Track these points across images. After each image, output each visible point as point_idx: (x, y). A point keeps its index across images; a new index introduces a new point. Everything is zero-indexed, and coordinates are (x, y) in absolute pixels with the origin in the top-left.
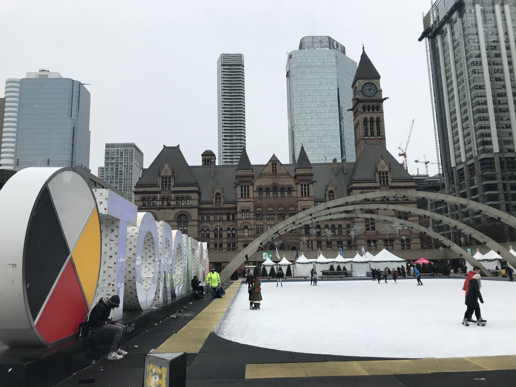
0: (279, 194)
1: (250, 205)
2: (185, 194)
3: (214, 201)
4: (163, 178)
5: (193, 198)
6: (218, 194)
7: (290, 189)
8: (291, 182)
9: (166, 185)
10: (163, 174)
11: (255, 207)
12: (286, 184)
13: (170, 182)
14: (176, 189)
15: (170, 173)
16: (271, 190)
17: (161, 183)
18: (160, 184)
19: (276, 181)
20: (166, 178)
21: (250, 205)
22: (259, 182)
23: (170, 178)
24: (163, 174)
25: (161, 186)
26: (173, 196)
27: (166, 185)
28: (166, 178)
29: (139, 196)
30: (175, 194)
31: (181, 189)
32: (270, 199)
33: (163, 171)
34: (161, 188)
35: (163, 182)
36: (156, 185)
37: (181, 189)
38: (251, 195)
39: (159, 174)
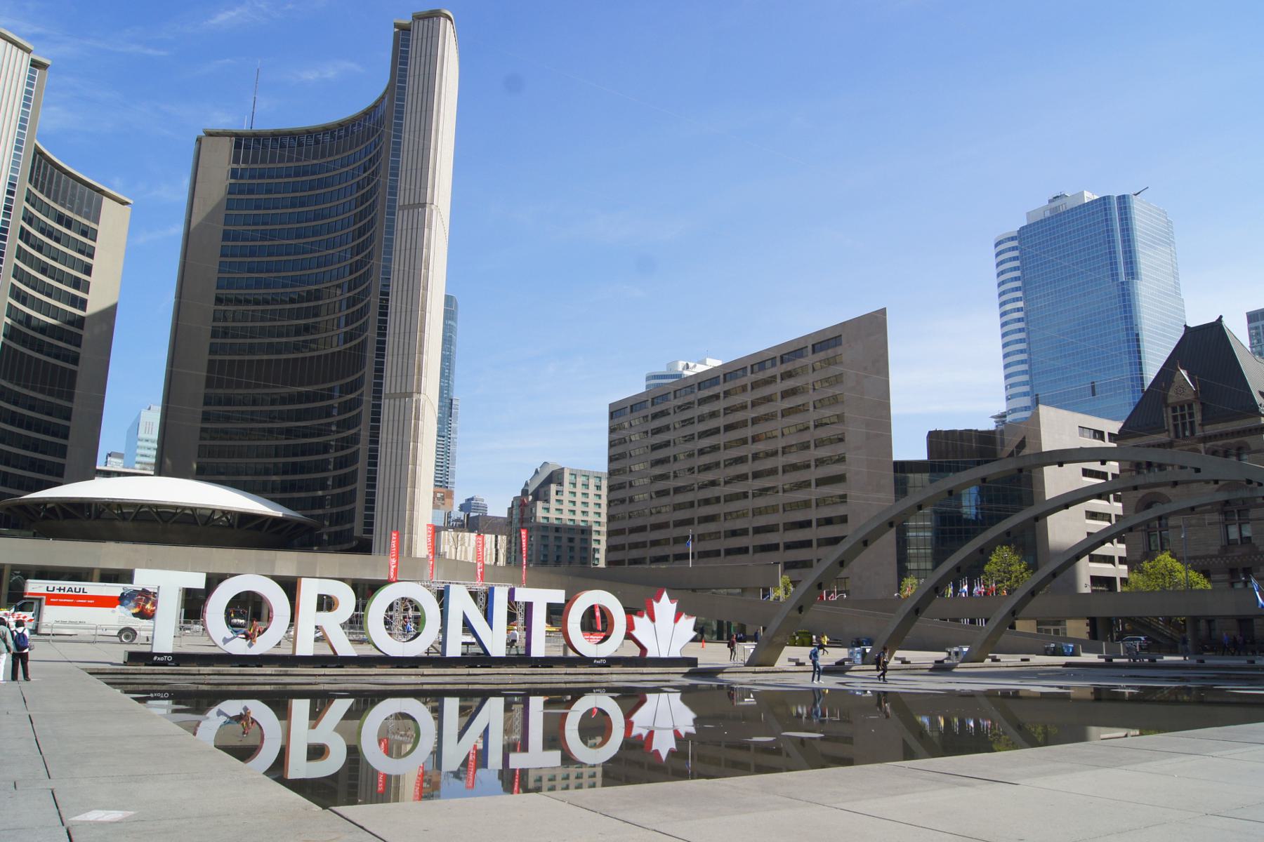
2: (1233, 441)
4: (1174, 410)
5: (1253, 448)
9: (1184, 425)
10: (1170, 401)
13: (1191, 415)
14: (1210, 429)
17: (1171, 421)
20: (1182, 408)
23: (1190, 406)
25: (1171, 428)
27: (1184, 425)
28: (1182, 408)
30: (1209, 445)
31: (1221, 427)
33: (1171, 393)
34: (1172, 434)
35: (1175, 418)
36: (1160, 428)
37: (1221, 427)
39: (1165, 398)
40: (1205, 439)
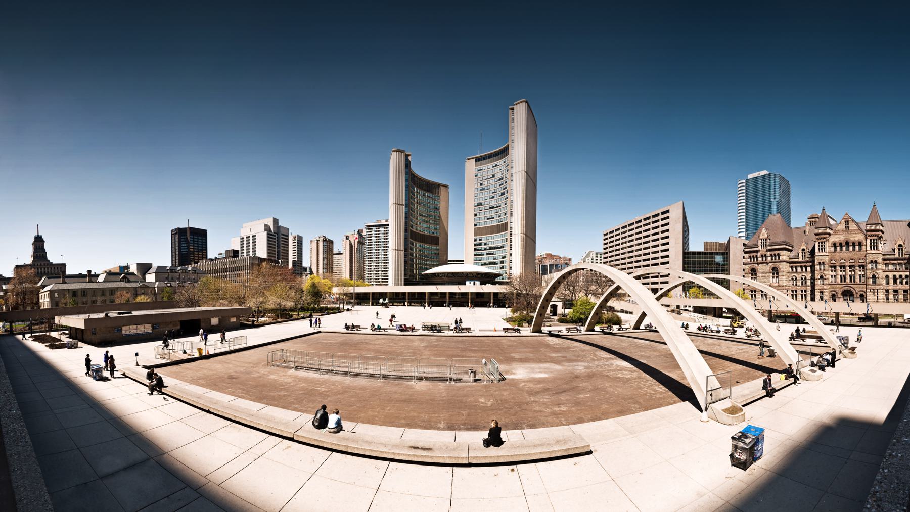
1: (826, 260)
3: (801, 255)
6: (803, 250)
8: (859, 237)
11: (830, 260)
12: (857, 239)
15: (766, 236)
16: (844, 244)
18: (760, 244)
21: (826, 260)
22: (833, 239)
24: (761, 237)
26: (769, 253)
29: (747, 256)
32: (844, 255)
38: (827, 250)
40: (770, 250)
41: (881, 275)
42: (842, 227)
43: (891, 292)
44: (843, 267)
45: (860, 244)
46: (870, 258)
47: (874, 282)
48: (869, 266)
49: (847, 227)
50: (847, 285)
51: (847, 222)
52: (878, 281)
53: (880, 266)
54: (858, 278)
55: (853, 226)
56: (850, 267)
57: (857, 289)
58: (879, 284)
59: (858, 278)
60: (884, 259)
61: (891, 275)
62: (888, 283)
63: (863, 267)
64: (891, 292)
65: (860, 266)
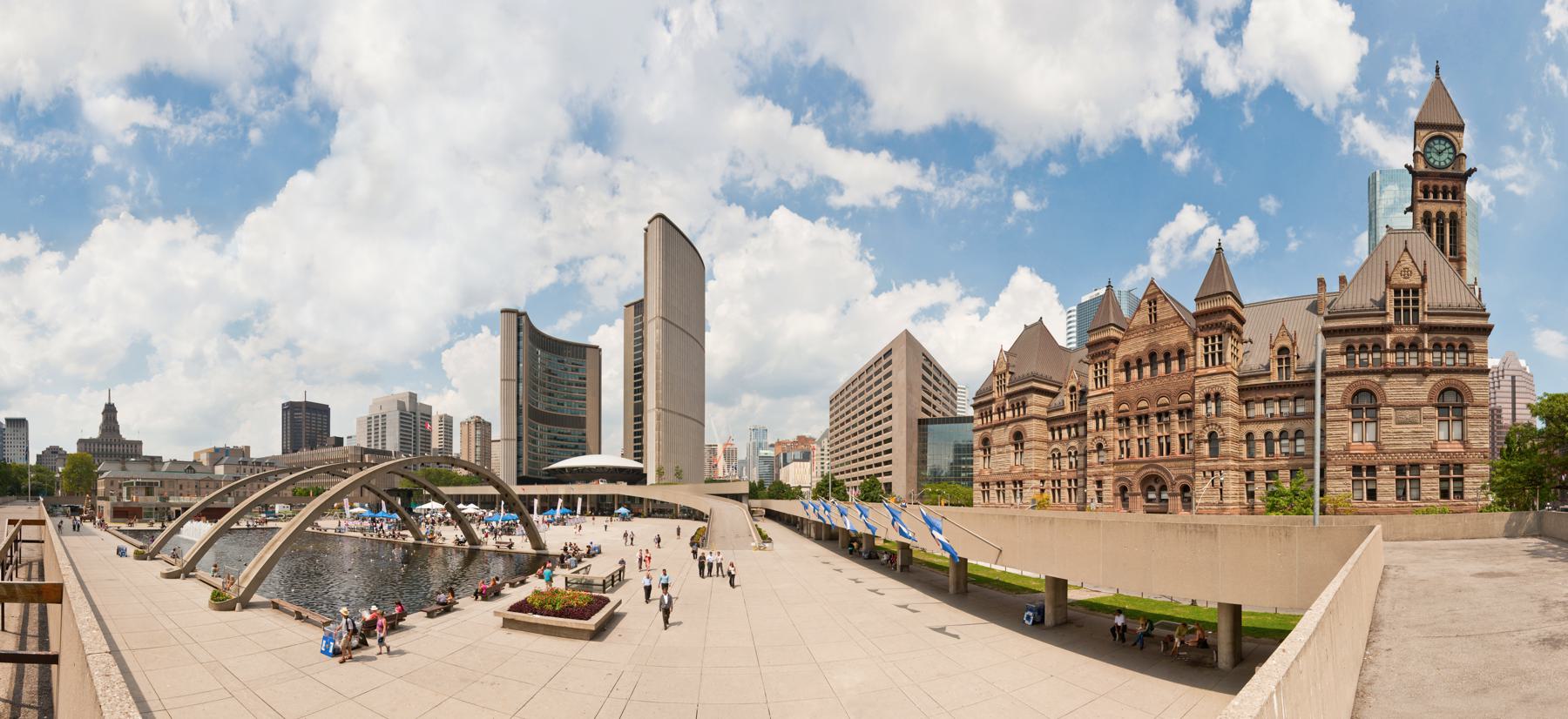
0: (1161, 368)
7: (1182, 354)
12: (1174, 341)
19: (1155, 338)
41: (1230, 427)
42: (1143, 317)
43: (1260, 476)
44: (1143, 418)
45: (1182, 354)
46: (1203, 386)
47: (1214, 452)
48: (1201, 410)
49: (1153, 316)
50: (1151, 464)
51: (1153, 302)
52: (1226, 448)
53: (1228, 407)
54: (1176, 442)
55: (1164, 313)
56: (1159, 415)
57: (1173, 472)
58: (1226, 457)
59: (1176, 442)
60: (1241, 390)
61: (1259, 431)
62: (1251, 455)
63: (1187, 413)
64: (1260, 476)
65: (1180, 413)
